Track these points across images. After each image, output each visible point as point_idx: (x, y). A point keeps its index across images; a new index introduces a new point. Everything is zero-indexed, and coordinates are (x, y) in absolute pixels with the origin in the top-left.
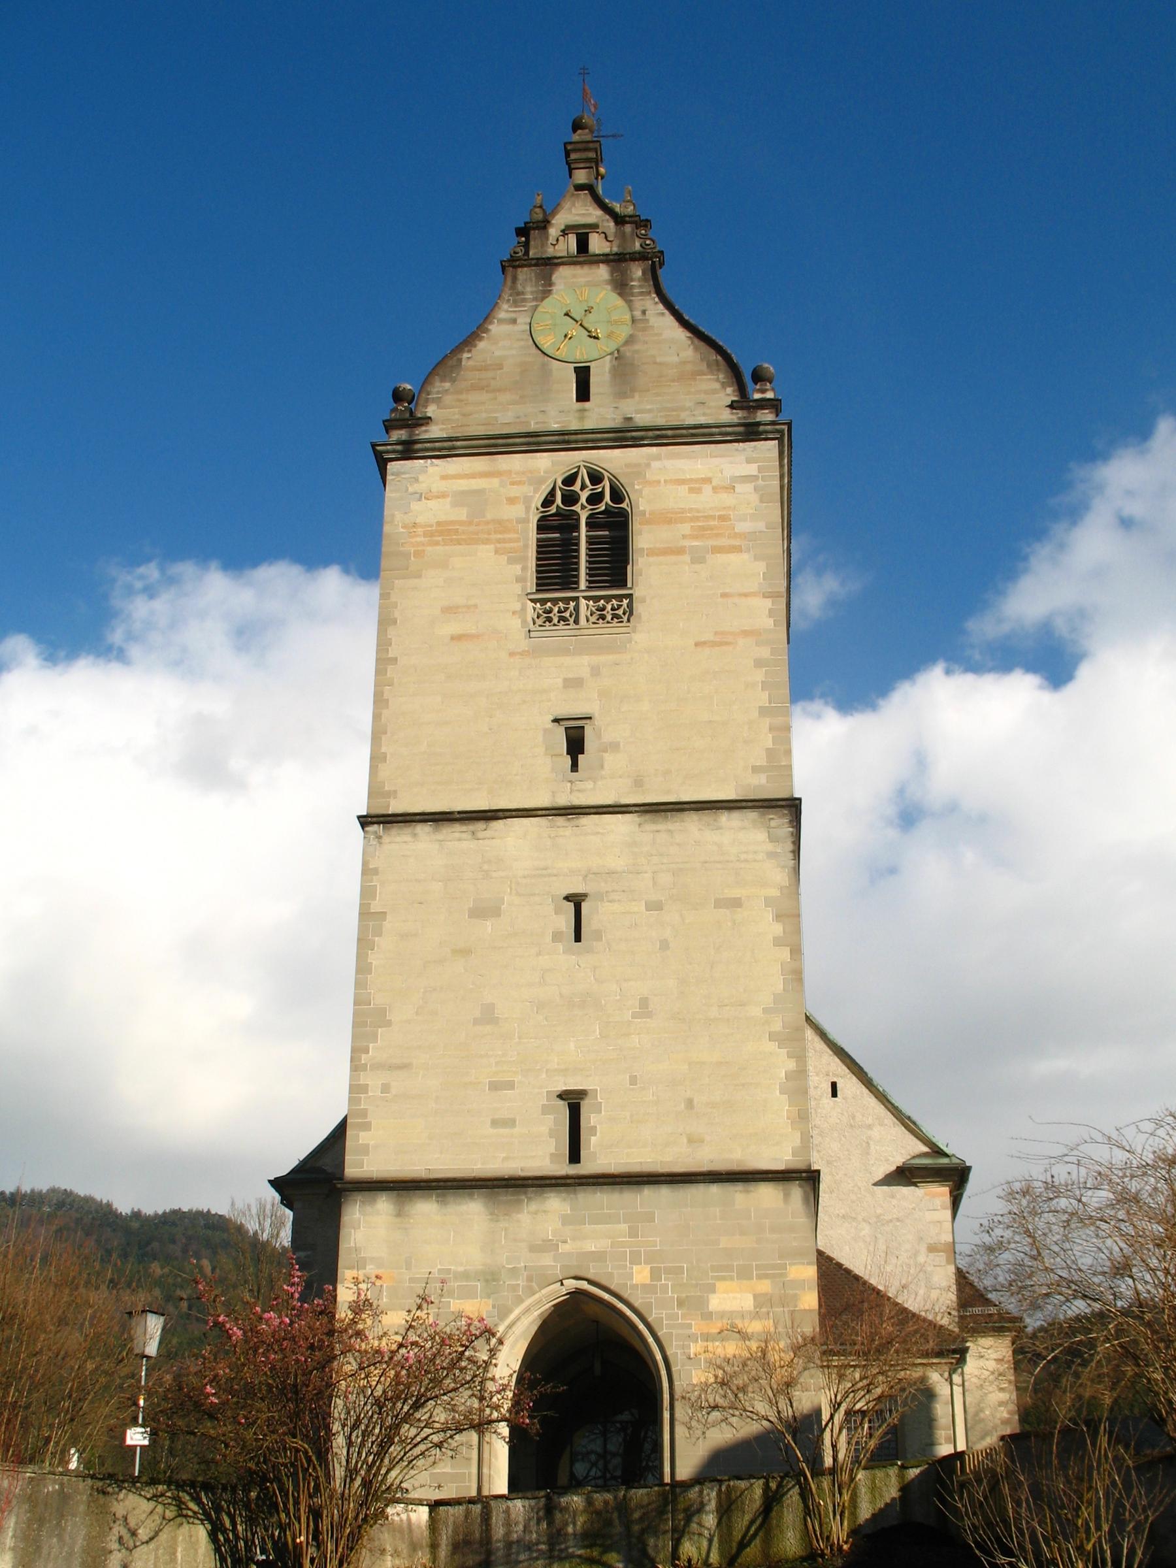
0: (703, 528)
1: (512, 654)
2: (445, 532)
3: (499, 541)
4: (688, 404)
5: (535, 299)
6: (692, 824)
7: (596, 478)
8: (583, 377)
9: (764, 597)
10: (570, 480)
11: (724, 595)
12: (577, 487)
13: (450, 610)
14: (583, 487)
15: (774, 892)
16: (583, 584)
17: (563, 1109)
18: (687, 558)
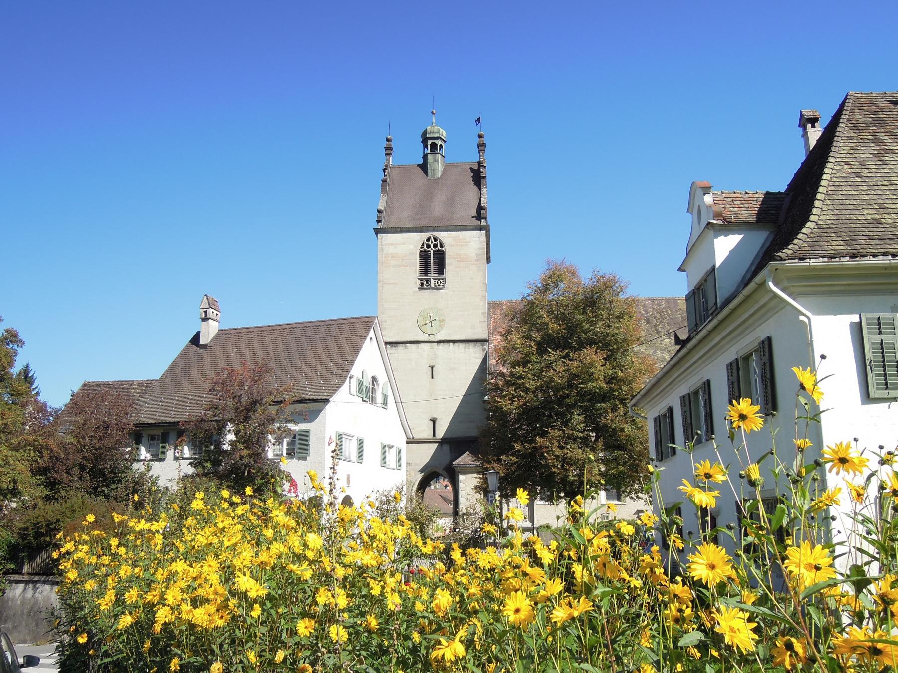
7: (435, 240)
10: (428, 240)
12: (430, 243)
14: (432, 243)
17: (431, 423)
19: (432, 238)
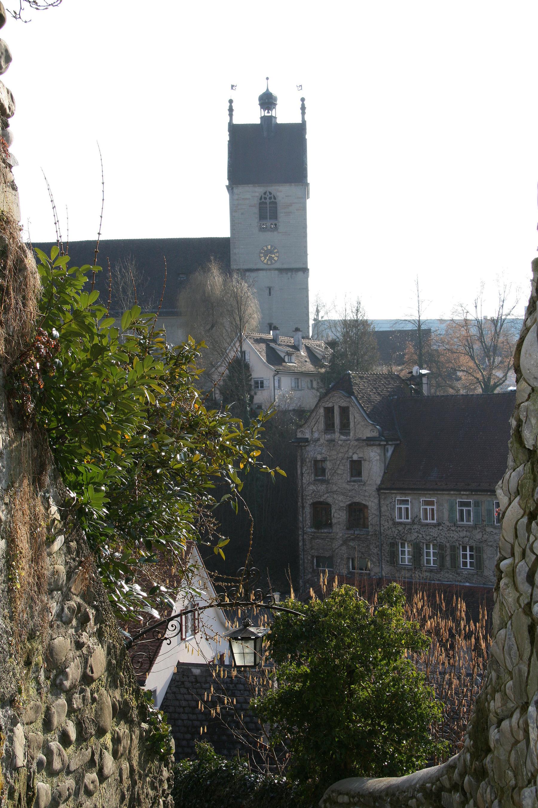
7: (270, 193)
10: (265, 193)
19: (268, 193)
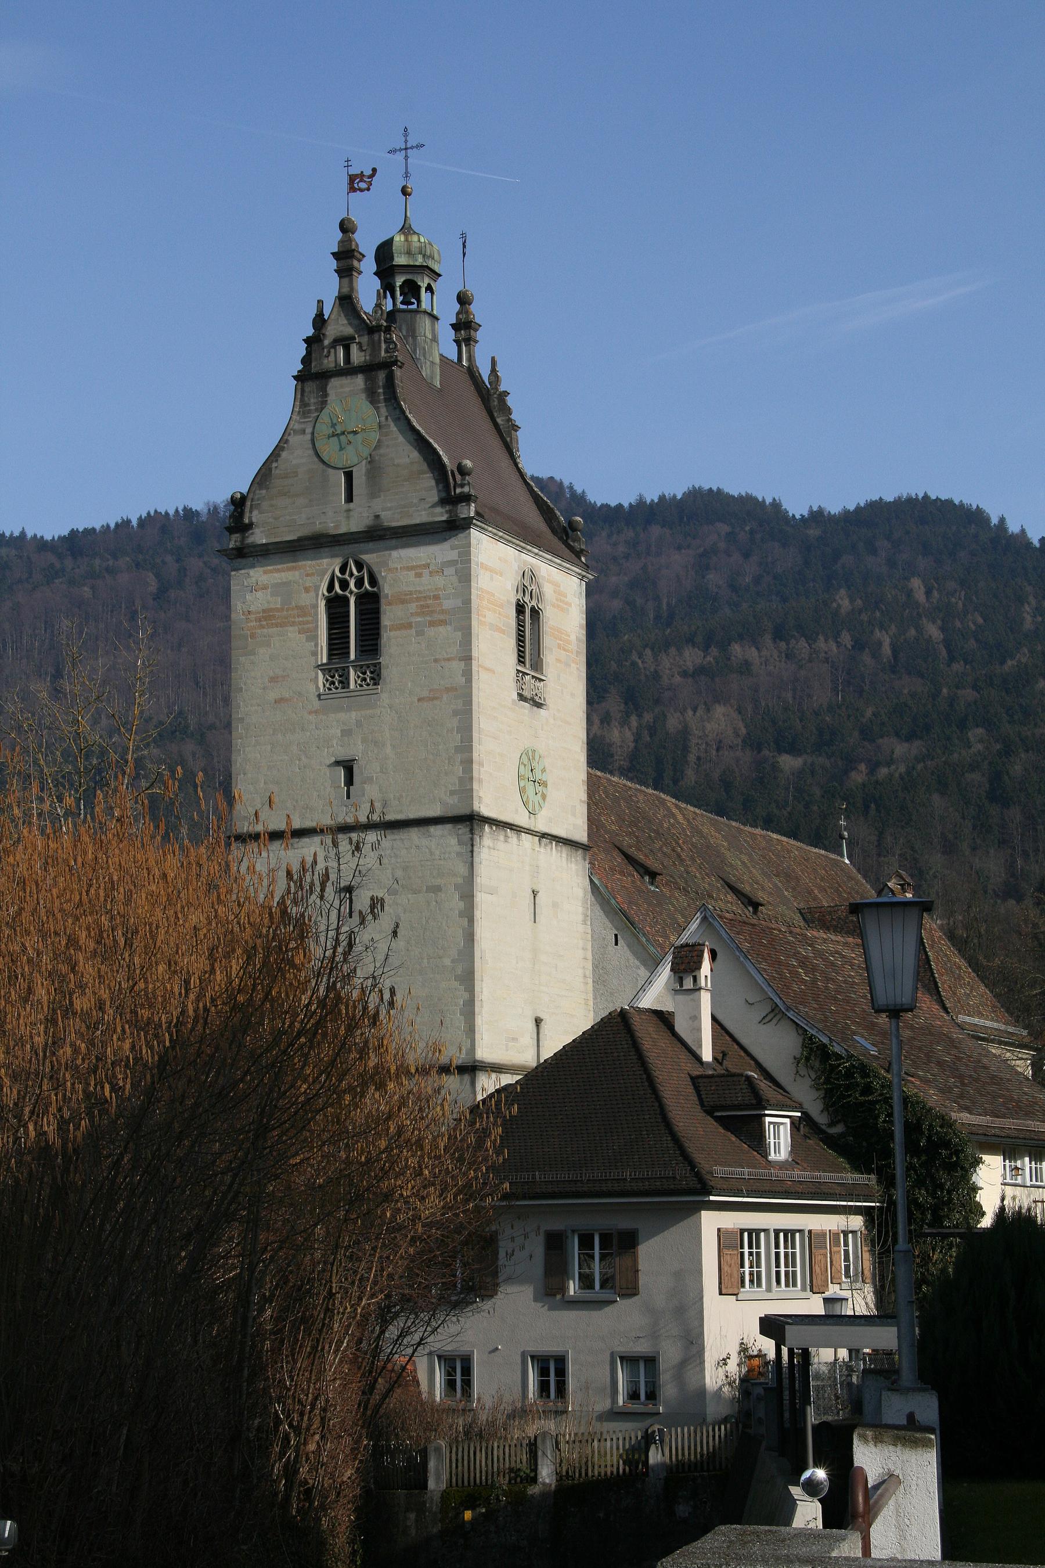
0: (422, 606)
1: (310, 713)
2: (267, 616)
3: (300, 623)
4: (415, 501)
5: (316, 410)
6: (414, 835)
8: (349, 476)
9: (460, 660)
11: (436, 661)
13: (273, 679)
15: (460, 880)
16: (352, 656)
18: (413, 631)
